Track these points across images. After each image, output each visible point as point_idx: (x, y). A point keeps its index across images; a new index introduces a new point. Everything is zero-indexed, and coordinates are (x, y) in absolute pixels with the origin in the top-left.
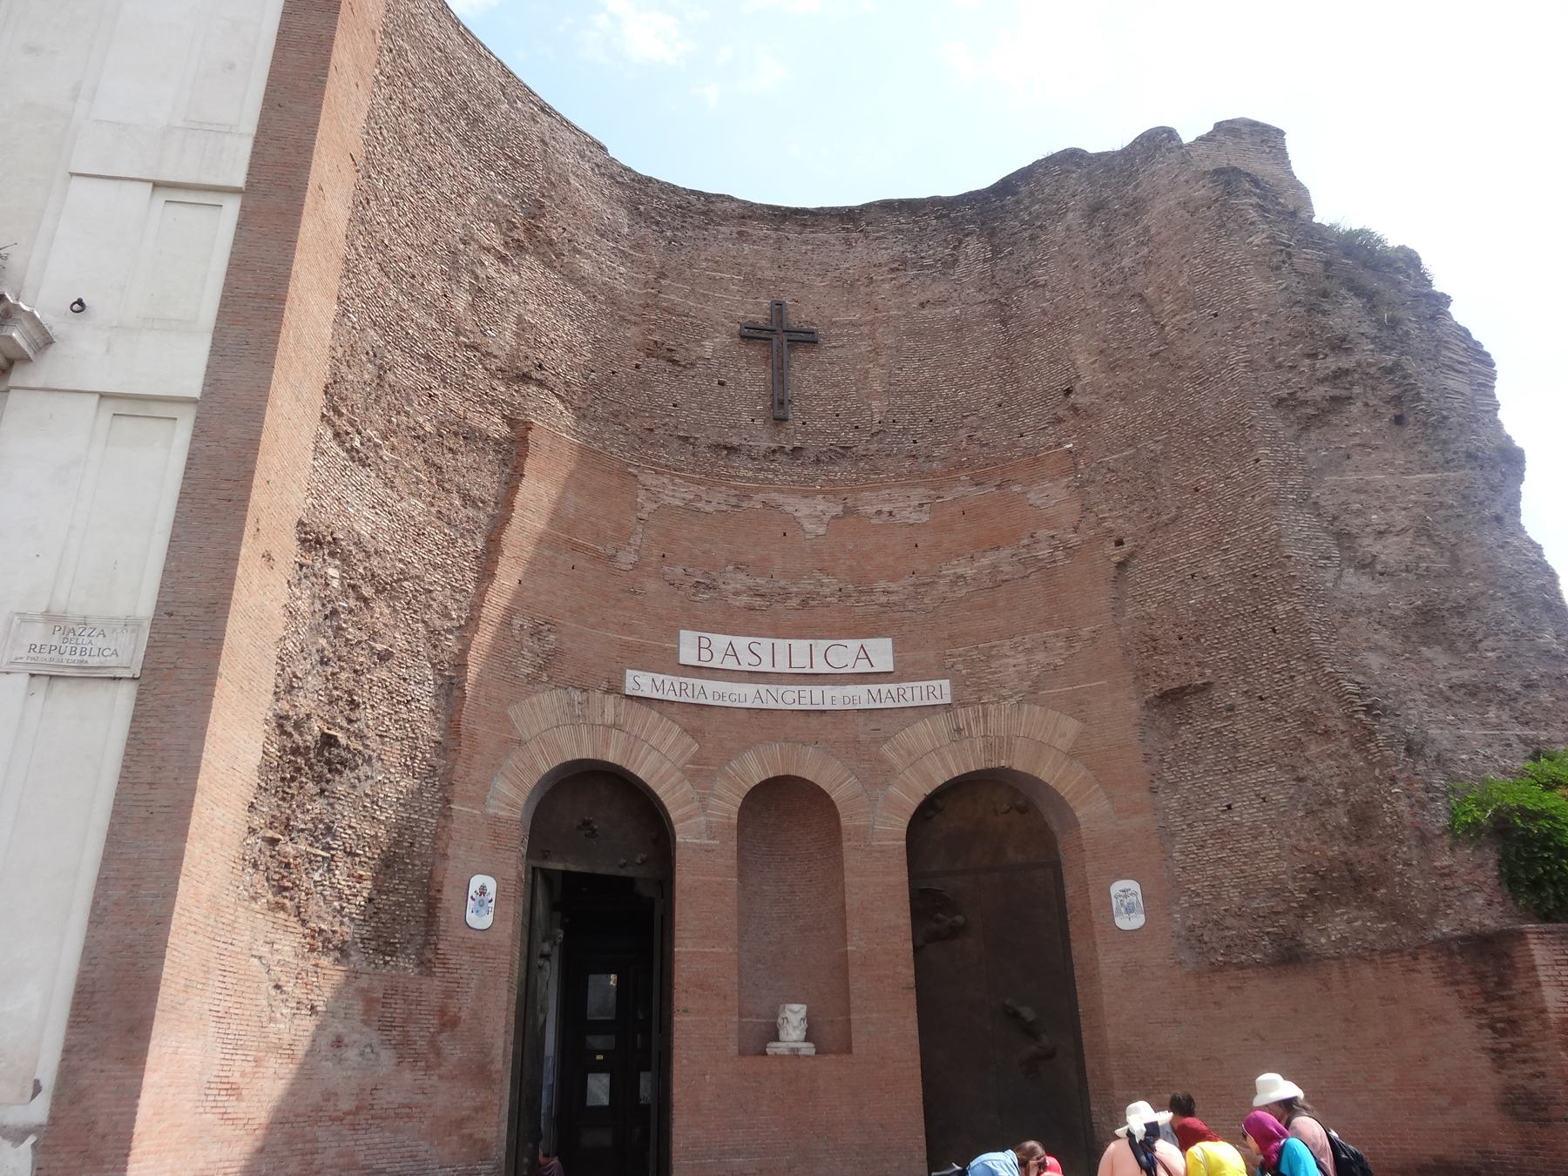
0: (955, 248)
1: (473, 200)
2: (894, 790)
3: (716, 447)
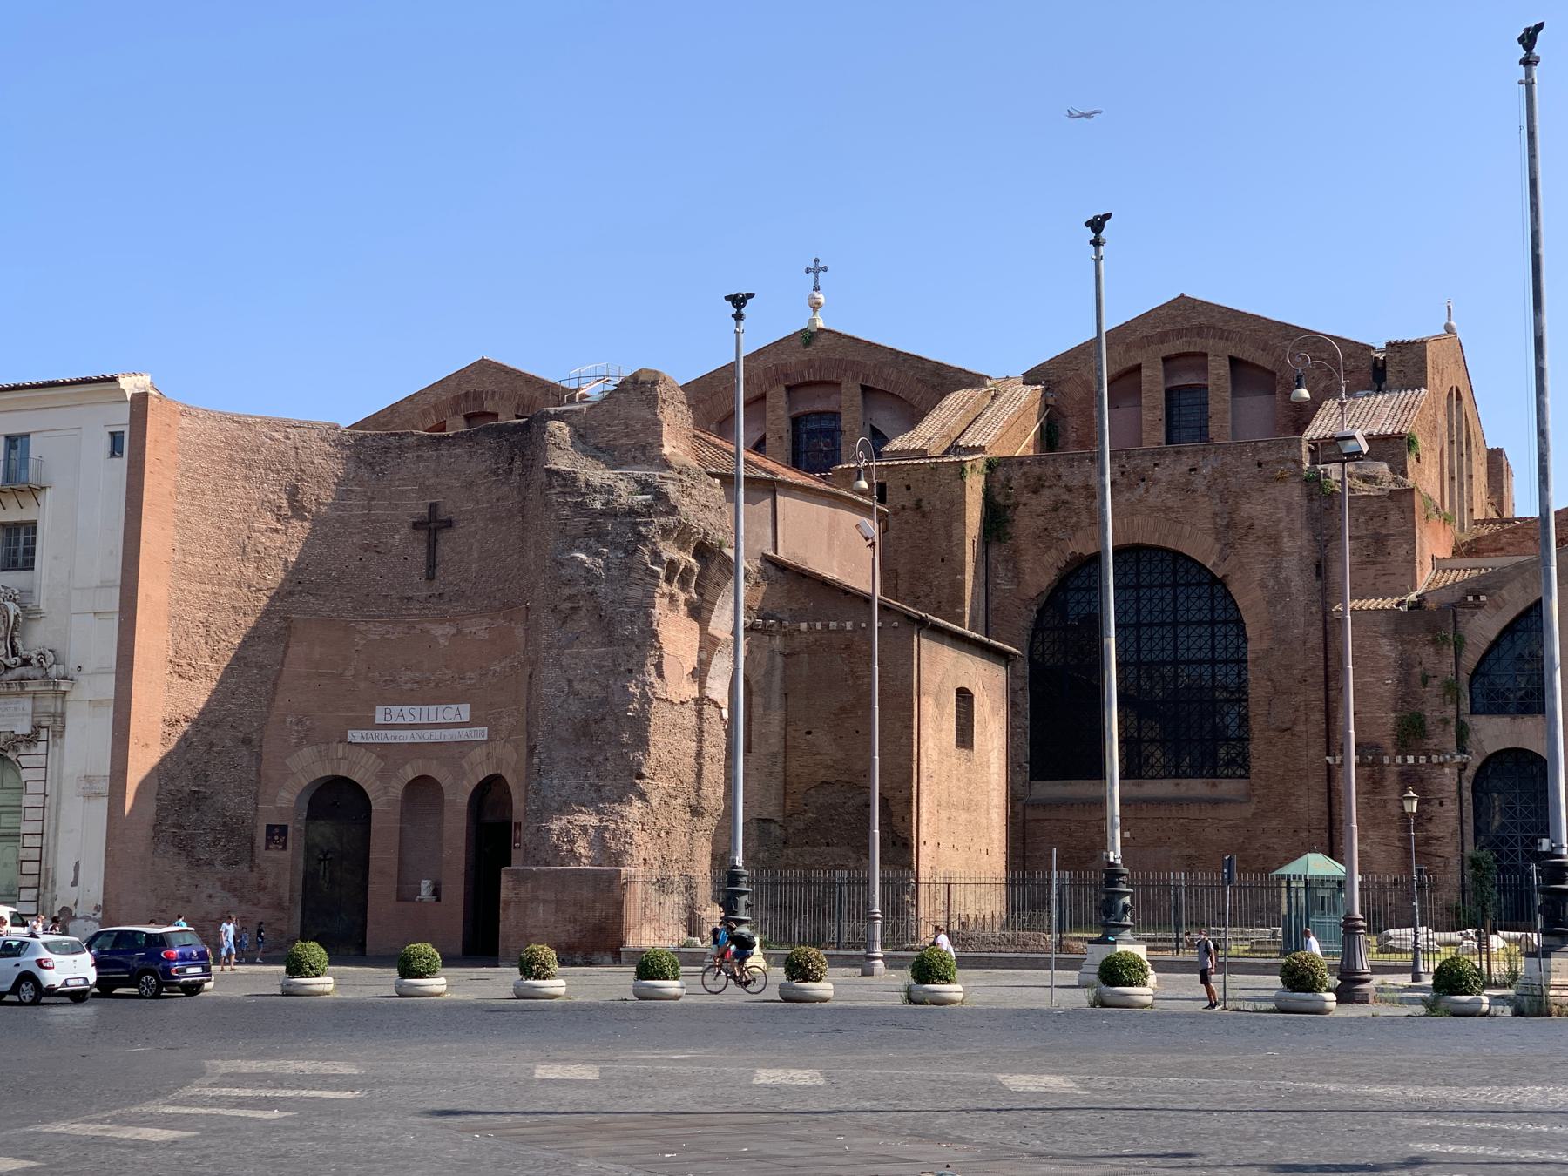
0: (510, 464)
1: (255, 508)
2: (465, 782)
3: (401, 599)
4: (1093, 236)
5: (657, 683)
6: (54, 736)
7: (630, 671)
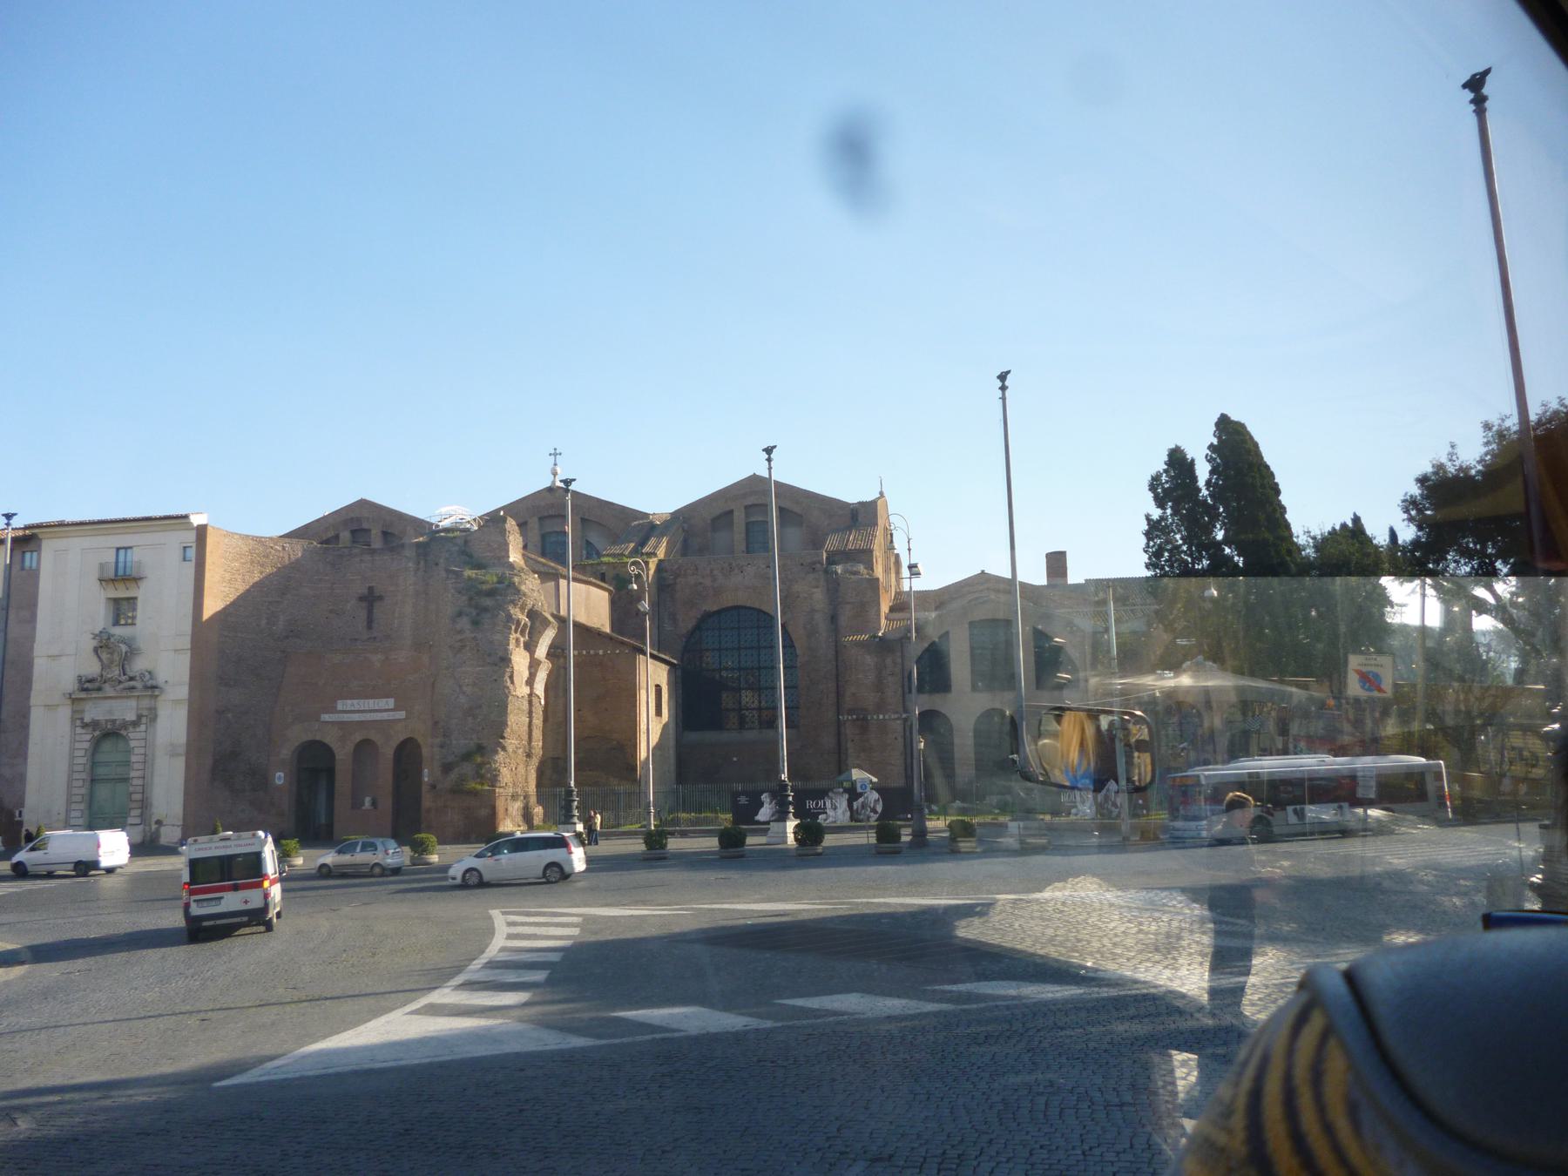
4: (767, 456)
5: (511, 687)
6: (150, 721)
7: (496, 680)
